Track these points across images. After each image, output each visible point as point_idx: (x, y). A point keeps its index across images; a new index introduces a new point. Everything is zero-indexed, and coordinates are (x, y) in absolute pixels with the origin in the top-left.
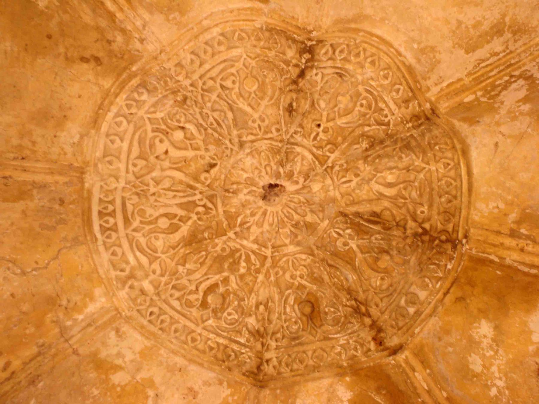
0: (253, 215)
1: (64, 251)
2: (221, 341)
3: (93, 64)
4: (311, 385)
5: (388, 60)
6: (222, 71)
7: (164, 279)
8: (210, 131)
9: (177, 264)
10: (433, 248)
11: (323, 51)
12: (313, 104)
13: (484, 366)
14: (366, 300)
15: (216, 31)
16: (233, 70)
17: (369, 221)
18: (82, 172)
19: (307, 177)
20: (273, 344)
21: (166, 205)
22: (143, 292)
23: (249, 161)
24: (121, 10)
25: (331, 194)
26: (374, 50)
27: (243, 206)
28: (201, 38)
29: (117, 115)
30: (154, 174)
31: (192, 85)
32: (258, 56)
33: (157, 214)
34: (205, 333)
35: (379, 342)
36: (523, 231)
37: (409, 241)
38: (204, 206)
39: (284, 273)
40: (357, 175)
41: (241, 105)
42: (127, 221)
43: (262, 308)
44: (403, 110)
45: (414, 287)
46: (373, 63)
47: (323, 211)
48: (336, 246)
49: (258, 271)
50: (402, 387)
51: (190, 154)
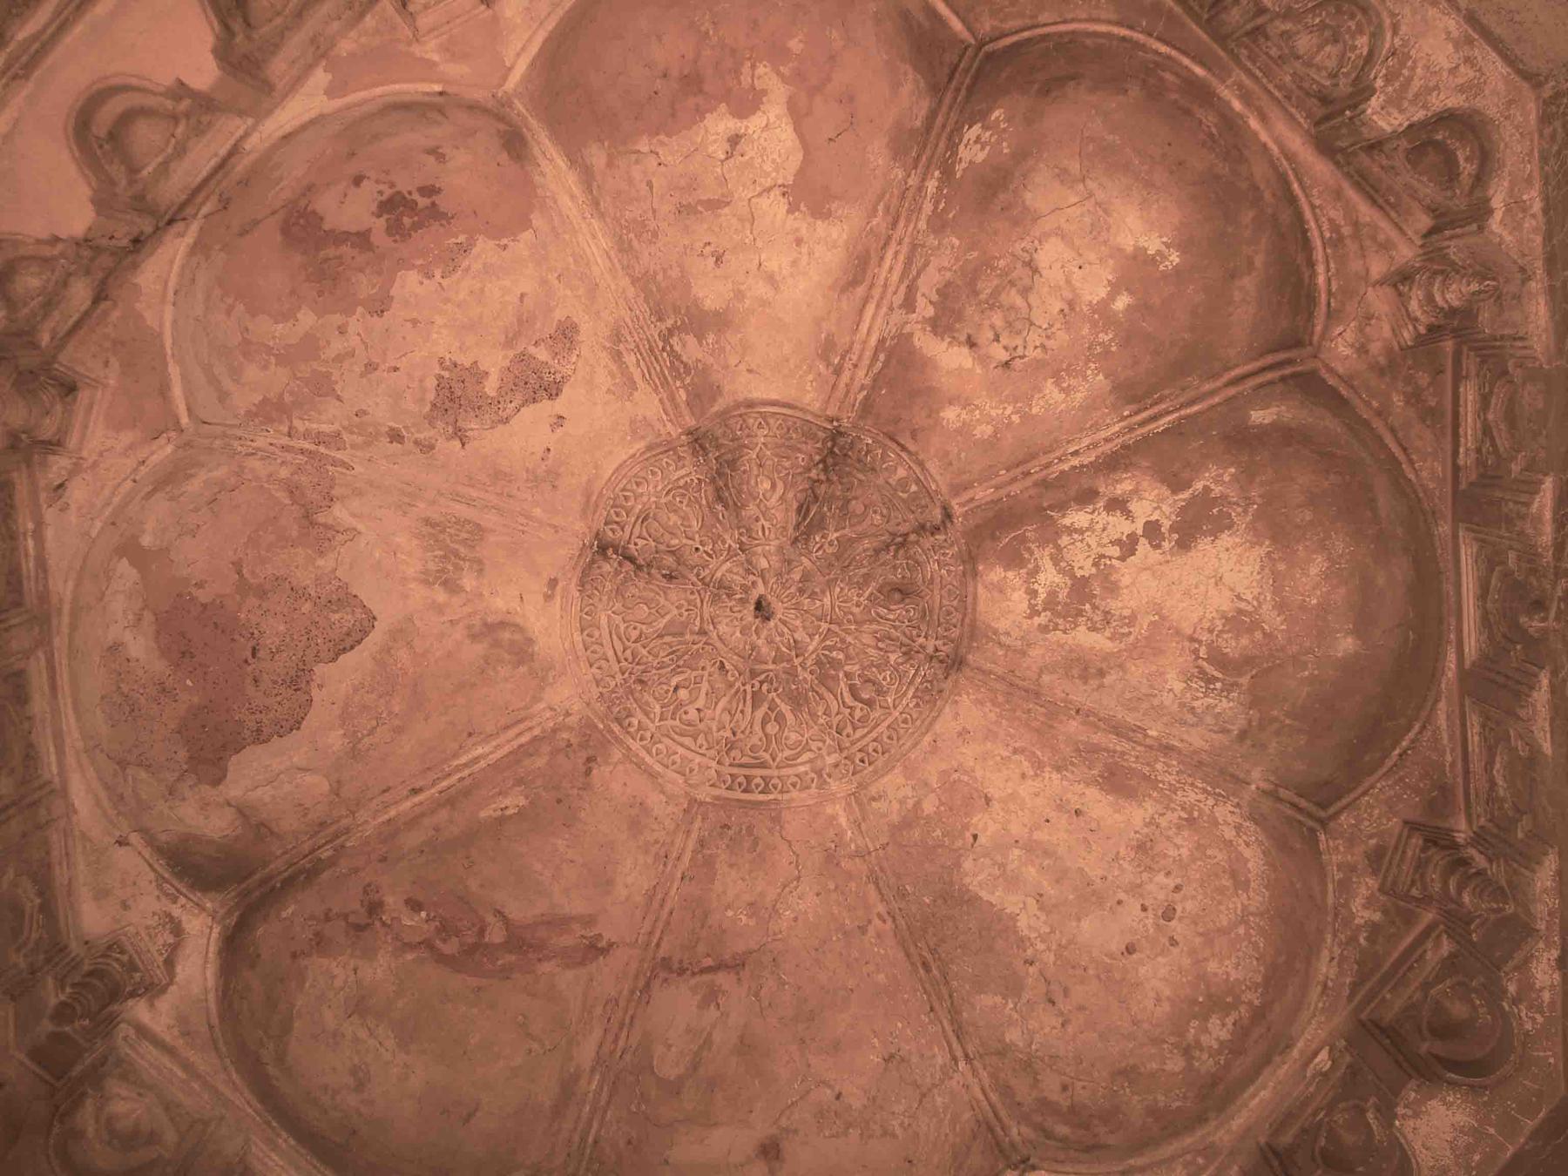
0: (782, 635)
1: (784, 833)
2: (910, 694)
3: (592, 764)
4: (981, 607)
5: (637, 468)
6: (620, 639)
7: (828, 741)
8: (681, 663)
9: (815, 723)
10: (846, 455)
11: (610, 534)
12: (672, 553)
13: (988, 423)
14: (890, 534)
15: (577, 638)
16: (622, 627)
17: (804, 519)
18: (693, 801)
19: (748, 572)
20: (921, 640)
21: (752, 724)
22: (836, 766)
23: (722, 628)
24: (531, 729)
25: (773, 549)
26: (625, 481)
27: (770, 641)
28: (580, 654)
29: (649, 752)
30: (714, 729)
31: (623, 674)
32: (609, 599)
33: (761, 734)
34: (900, 708)
35: (936, 530)
36: (836, 361)
37: (835, 478)
38: (761, 683)
39: (852, 613)
40: (757, 520)
41: (661, 625)
42: (763, 765)
43: (881, 645)
44: (686, 463)
45: (891, 481)
46: (638, 484)
47: (789, 562)
48: (833, 554)
49: (843, 641)
50: (991, 514)
51: (705, 686)
